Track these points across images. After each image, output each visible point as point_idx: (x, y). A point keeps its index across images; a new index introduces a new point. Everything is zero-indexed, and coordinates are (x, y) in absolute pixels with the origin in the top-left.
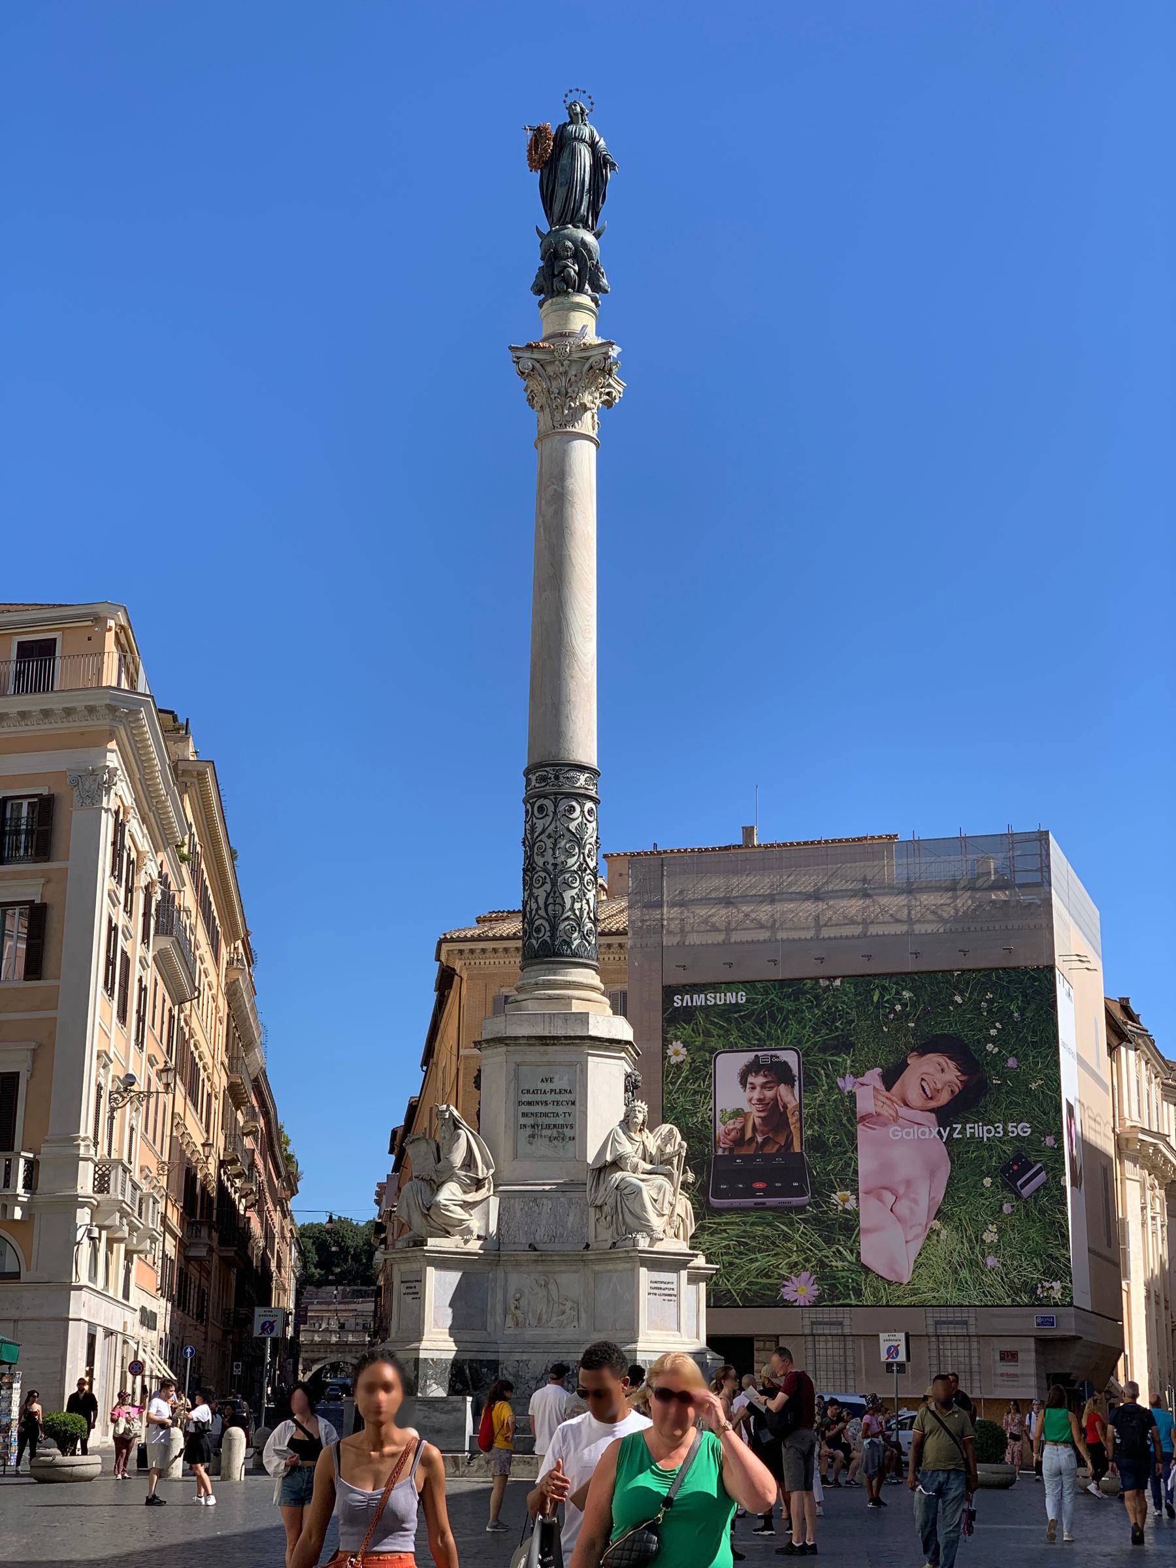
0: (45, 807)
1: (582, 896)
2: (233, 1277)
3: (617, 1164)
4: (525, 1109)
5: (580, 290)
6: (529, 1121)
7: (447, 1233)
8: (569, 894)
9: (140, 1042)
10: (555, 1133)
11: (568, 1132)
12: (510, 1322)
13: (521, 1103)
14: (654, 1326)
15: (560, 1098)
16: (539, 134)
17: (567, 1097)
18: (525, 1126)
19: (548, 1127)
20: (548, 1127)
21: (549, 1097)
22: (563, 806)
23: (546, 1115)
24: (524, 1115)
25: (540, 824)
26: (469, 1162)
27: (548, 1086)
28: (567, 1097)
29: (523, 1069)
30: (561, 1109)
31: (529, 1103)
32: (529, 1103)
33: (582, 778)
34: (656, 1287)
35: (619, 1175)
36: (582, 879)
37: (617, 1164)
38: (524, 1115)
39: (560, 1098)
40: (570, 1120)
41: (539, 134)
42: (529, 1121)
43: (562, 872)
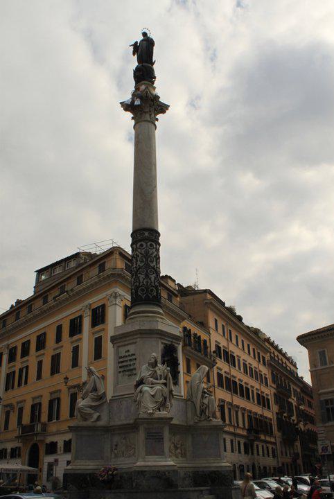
1: (147, 276)
4: (121, 365)
6: (122, 369)
7: (86, 420)
8: (142, 277)
10: (129, 373)
11: (134, 372)
12: (113, 456)
13: (119, 363)
14: (149, 453)
15: (131, 358)
17: (134, 357)
18: (120, 372)
19: (128, 371)
20: (128, 371)
21: (128, 358)
22: (138, 245)
23: (127, 366)
24: (120, 367)
27: (127, 354)
28: (134, 357)
29: (120, 349)
30: (132, 363)
31: (122, 362)
32: (122, 362)
33: (146, 234)
36: (147, 271)
38: (120, 367)
39: (131, 358)
40: (134, 367)
42: (122, 369)
43: (139, 269)
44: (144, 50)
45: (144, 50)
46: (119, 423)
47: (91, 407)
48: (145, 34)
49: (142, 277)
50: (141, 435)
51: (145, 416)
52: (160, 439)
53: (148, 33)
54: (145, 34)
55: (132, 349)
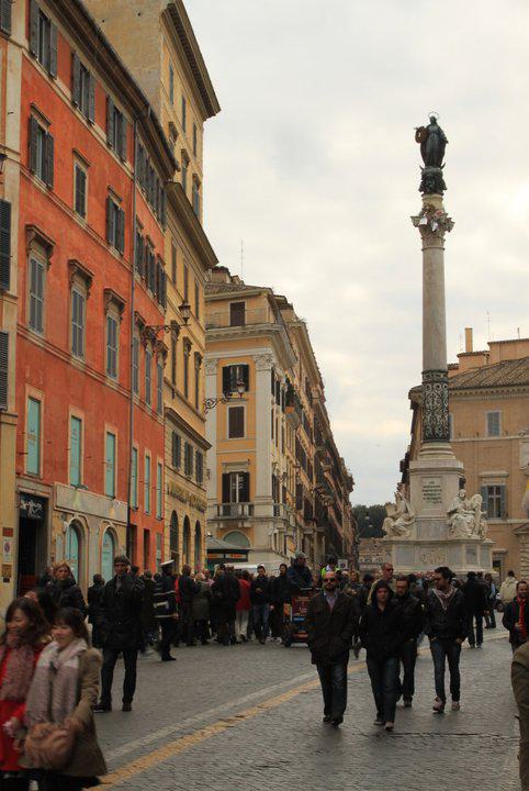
0: (245, 370)
2: (323, 540)
3: (455, 511)
5: (435, 192)
7: (400, 535)
8: (439, 417)
9: (283, 452)
14: (468, 563)
16: (419, 130)
25: (428, 393)
26: (407, 511)
29: (424, 480)
34: (469, 552)
35: (455, 515)
37: (455, 511)
41: (419, 130)
44: (432, 143)
45: (432, 143)
46: (429, 539)
47: (406, 526)
48: (433, 121)
49: (439, 417)
50: (464, 547)
51: (466, 538)
52: (475, 554)
53: (436, 117)
54: (433, 121)
55: (437, 482)
